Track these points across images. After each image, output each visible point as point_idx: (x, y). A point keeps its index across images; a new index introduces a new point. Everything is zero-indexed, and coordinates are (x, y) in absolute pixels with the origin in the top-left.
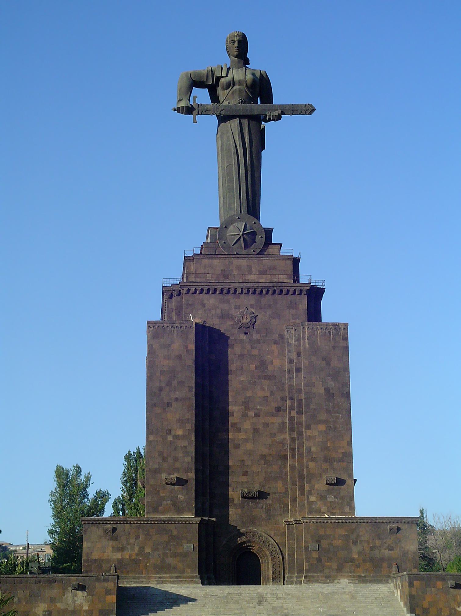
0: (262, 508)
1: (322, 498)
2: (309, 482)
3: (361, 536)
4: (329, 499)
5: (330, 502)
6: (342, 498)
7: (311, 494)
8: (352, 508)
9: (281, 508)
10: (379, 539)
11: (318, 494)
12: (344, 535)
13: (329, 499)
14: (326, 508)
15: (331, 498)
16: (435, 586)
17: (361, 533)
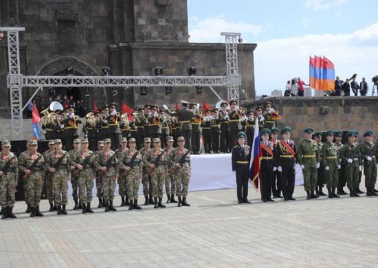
0: (83, 33)
1: (153, 21)
2: (139, 4)
3: (196, 64)
4: (160, 23)
5: (162, 26)
6: (175, 22)
7: (140, 17)
8: (186, 35)
9: (103, 33)
10: (214, 67)
11: (148, 17)
12: (178, 63)
13: (160, 23)
14: (157, 33)
15: (162, 22)
16: (306, 113)
17: (196, 62)
